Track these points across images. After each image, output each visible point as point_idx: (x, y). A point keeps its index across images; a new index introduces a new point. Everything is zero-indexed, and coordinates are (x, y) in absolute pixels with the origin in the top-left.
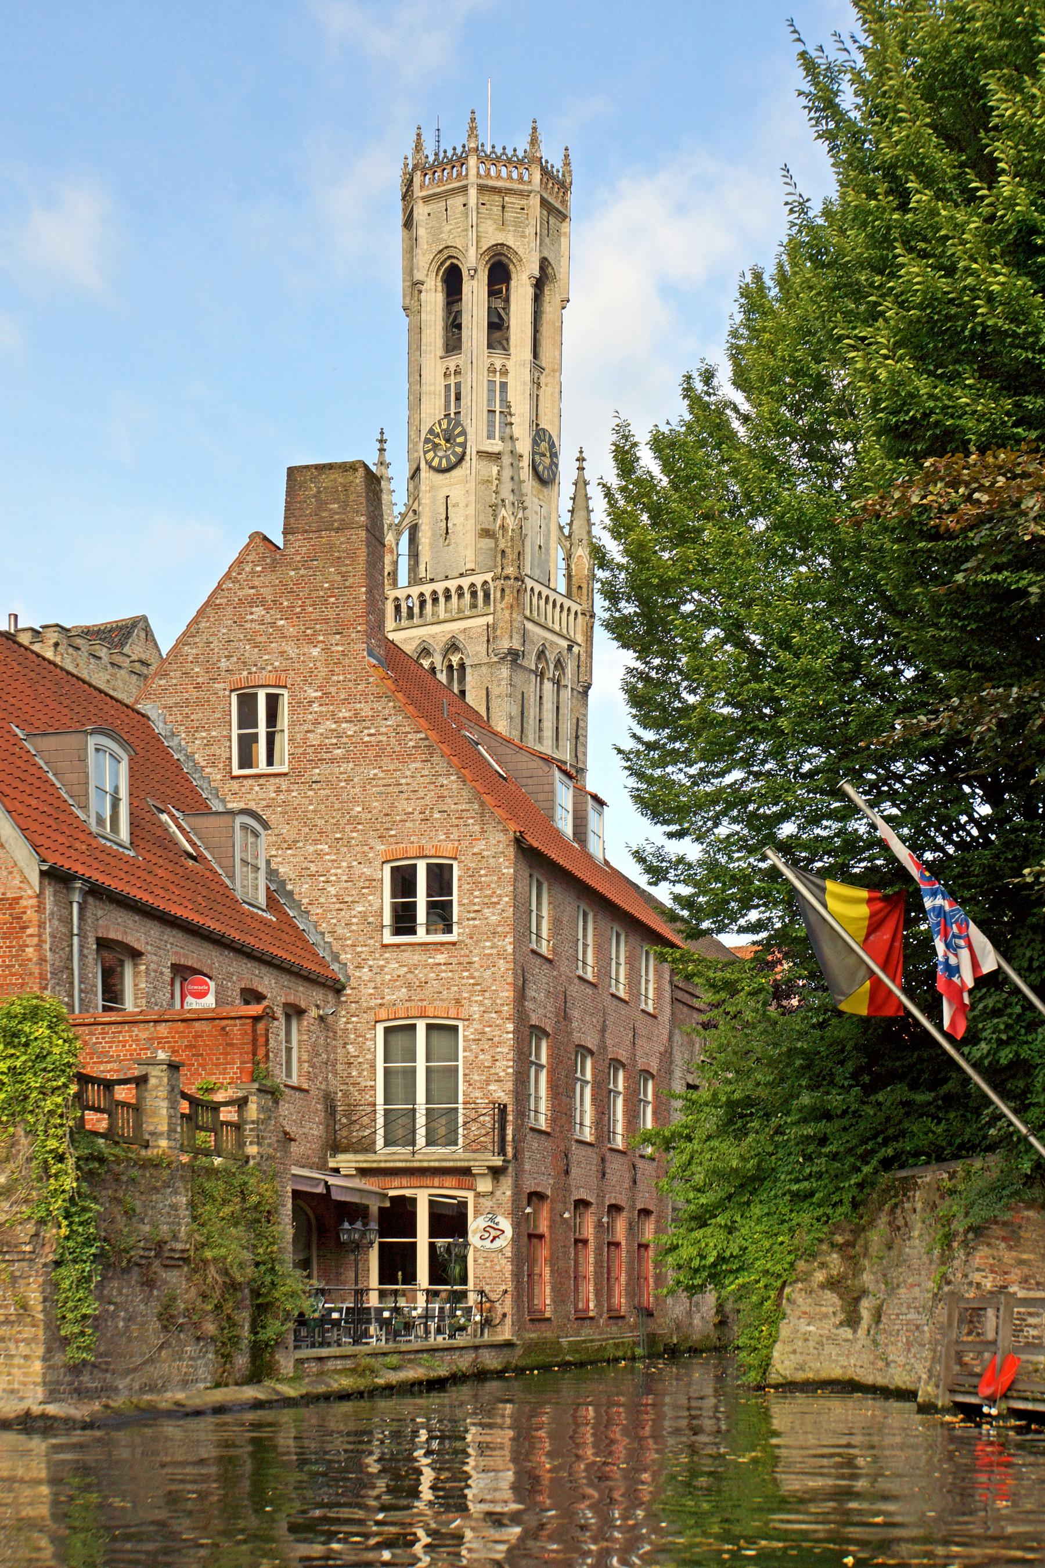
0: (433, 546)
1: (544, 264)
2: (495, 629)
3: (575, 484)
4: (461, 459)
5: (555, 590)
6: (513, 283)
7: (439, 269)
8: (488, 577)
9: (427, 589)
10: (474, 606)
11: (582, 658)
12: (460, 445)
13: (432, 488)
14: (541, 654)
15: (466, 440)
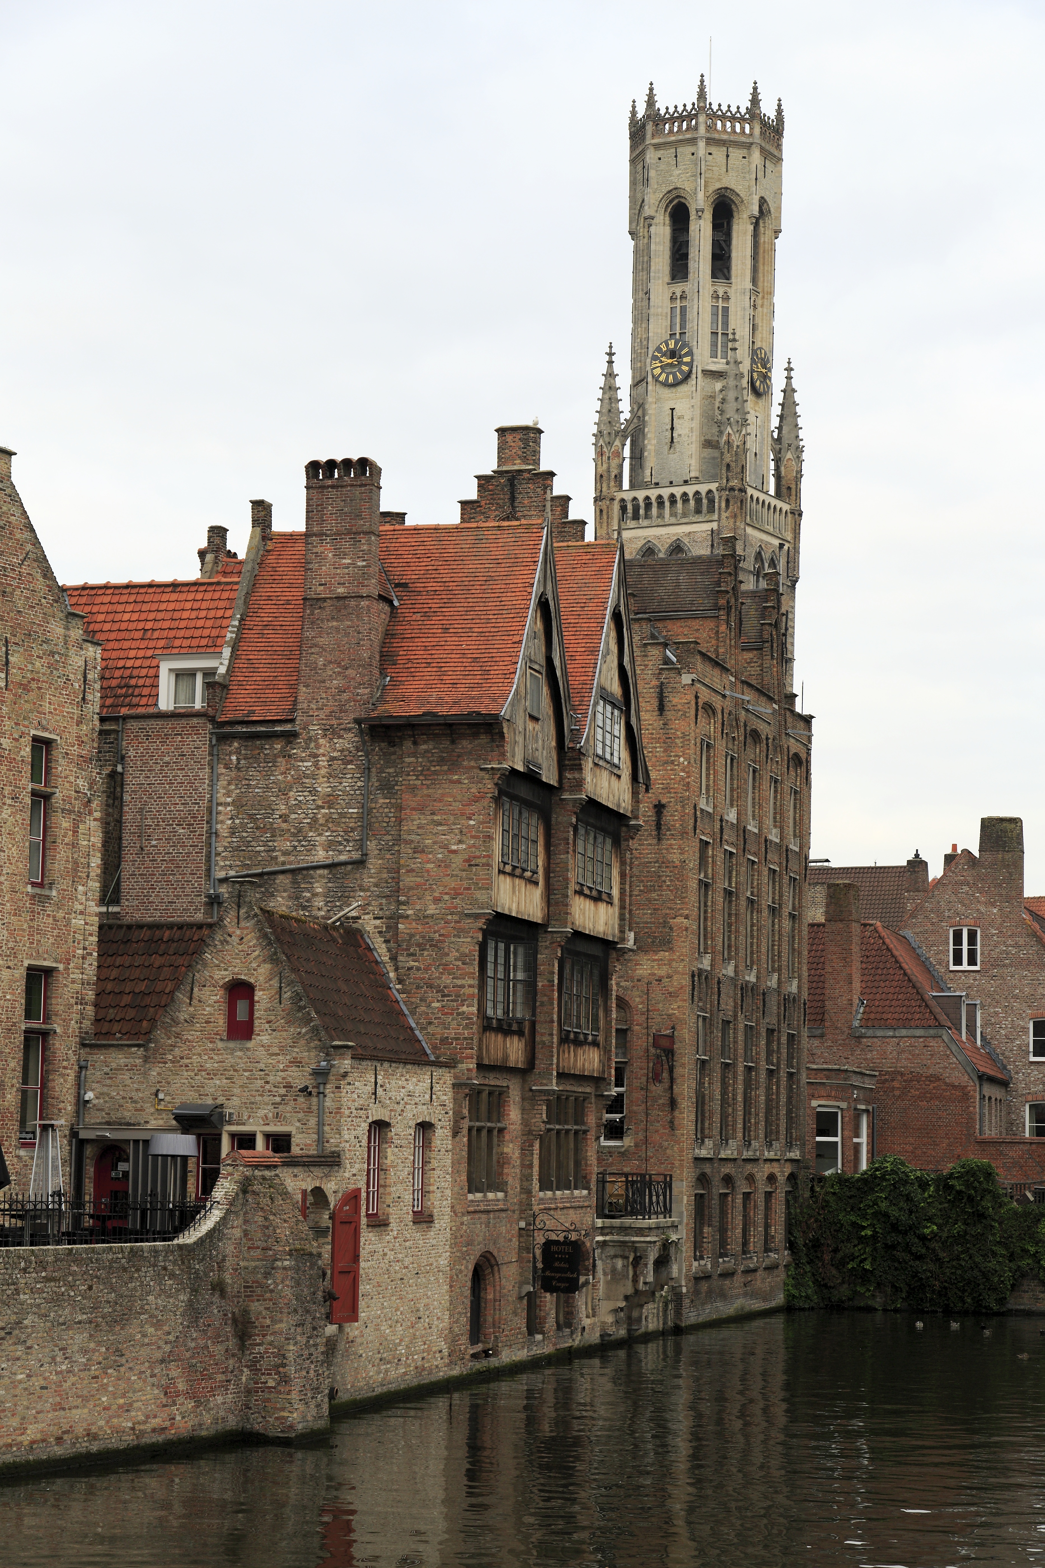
0: (658, 453)
1: (763, 201)
3: (784, 391)
4: (687, 377)
5: (766, 493)
6: (735, 221)
7: (667, 206)
8: (713, 486)
9: (653, 494)
10: (698, 511)
11: (791, 554)
12: (686, 364)
13: (658, 400)
14: (759, 556)
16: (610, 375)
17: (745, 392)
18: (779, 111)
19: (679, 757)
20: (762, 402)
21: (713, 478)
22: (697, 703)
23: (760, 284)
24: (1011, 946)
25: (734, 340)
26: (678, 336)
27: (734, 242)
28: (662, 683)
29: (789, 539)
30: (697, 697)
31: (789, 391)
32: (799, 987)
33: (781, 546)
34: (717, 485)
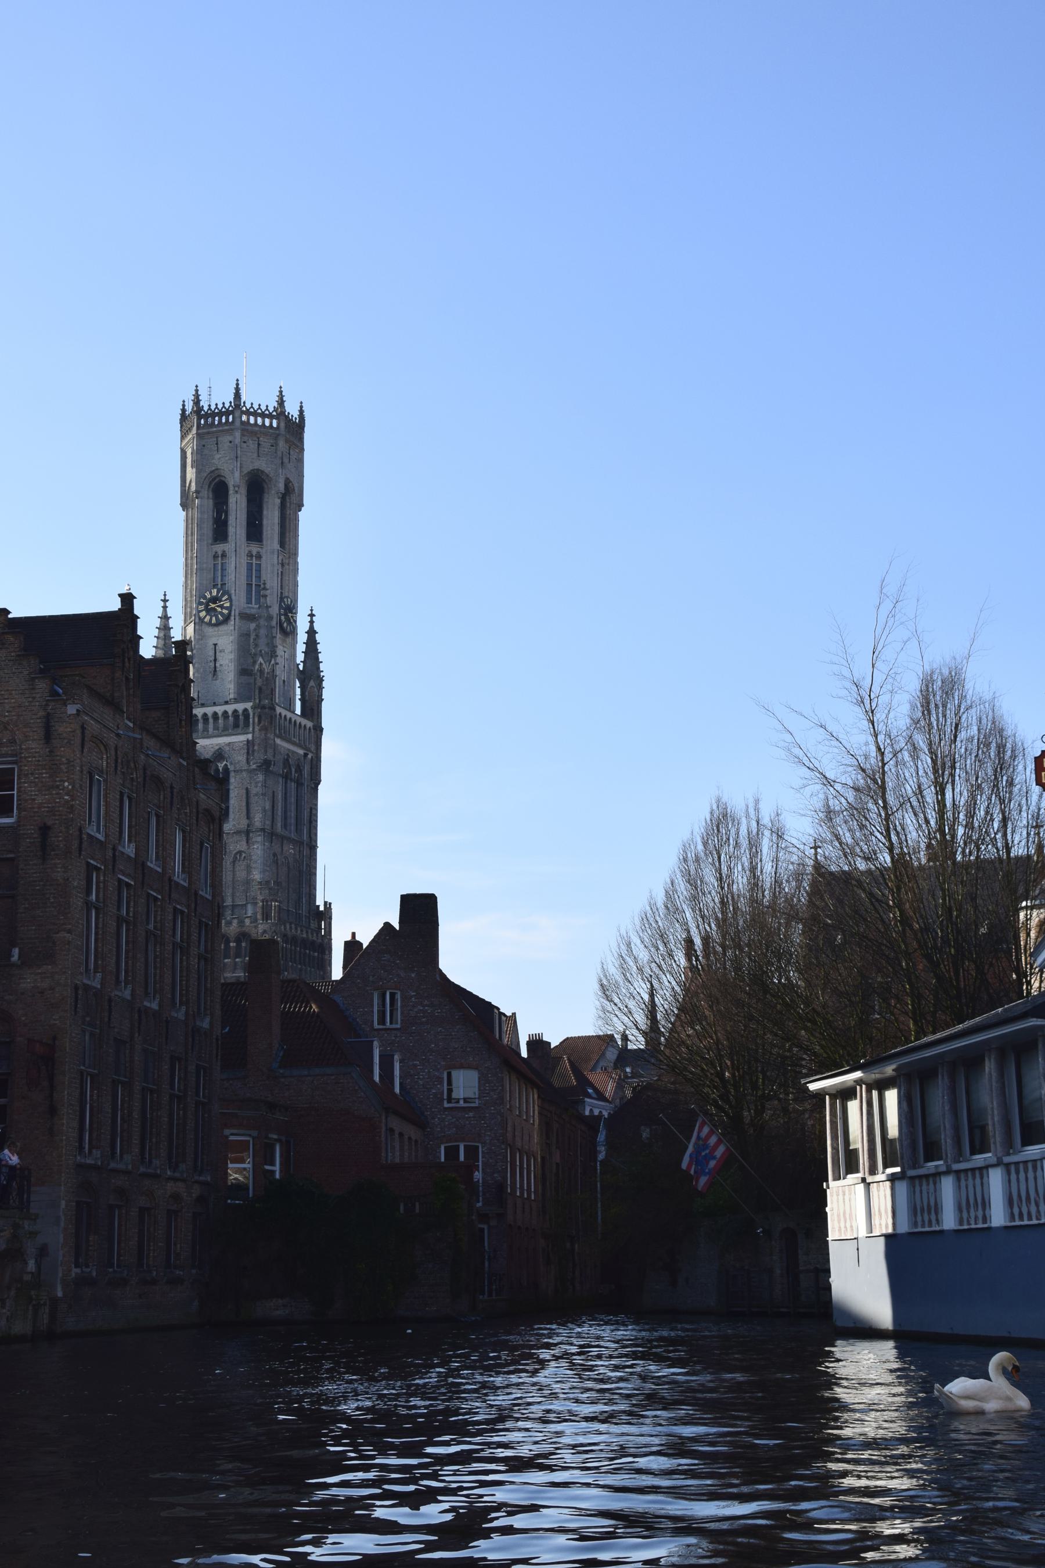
2: (254, 746)
4: (227, 619)
6: (266, 495)
7: (210, 483)
8: (248, 705)
10: (236, 725)
11: (314, 762)
12: (226, 608)
14: (286, 762)
15: (231, 605)
16: (165, 618)
17: (274, 631)
18: (301, 412)
19: (64, 781)
20: (289, 640)
21: (247, 699)
22: (83, 733)
23: (286, 546)
24: (426, 1005)
25: (267, 590)
26: (219, 586)
27: (265, 512)
28: (48, 714)
29: (312, 750)
30: (83, 728)
31: (312, 633)
32: (211, 1024)
33: (306, 755)
34: (251, 704)
